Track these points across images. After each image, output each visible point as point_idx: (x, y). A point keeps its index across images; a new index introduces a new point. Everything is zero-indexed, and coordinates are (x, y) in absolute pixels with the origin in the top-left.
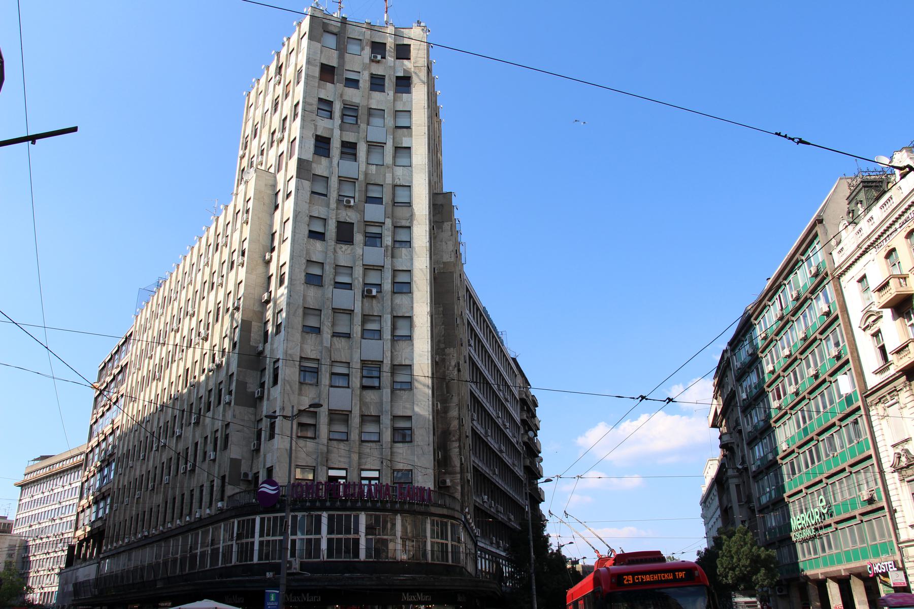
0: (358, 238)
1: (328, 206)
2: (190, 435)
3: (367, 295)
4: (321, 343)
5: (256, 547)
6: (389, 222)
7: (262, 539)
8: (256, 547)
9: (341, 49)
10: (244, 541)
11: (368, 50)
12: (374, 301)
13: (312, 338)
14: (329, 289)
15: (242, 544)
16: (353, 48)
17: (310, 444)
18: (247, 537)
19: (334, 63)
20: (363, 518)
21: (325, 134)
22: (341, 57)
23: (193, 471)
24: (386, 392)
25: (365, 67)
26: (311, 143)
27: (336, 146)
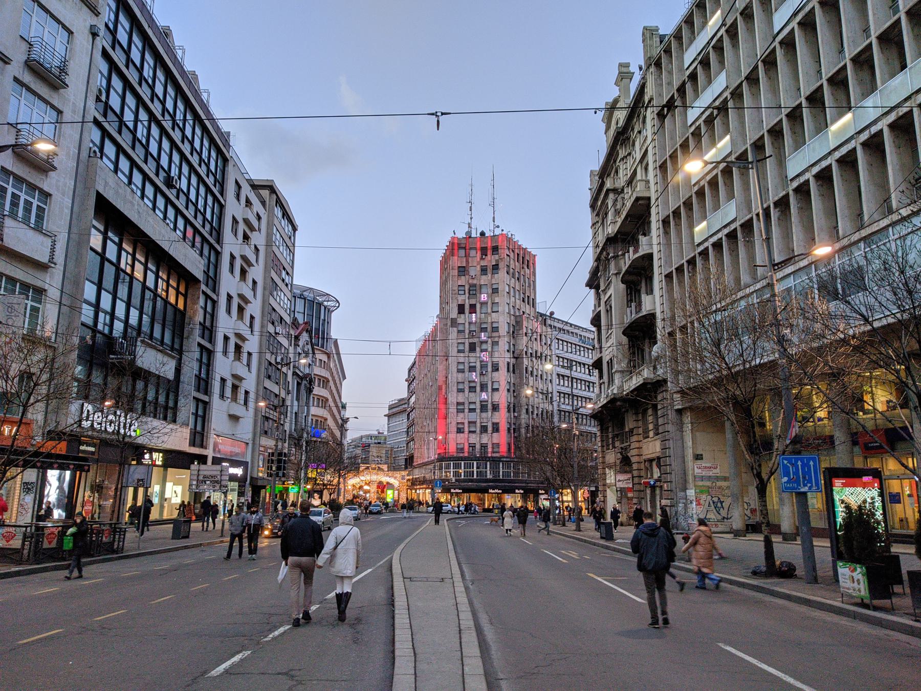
0: (478, 349)
3: (482, 374)
9: (467, 256)
11: (479, 253)
13: (461, 394)
14: (467, 373)
16: (473, 253)
19: (464, 265)
20: (475, 463)
22: (467, 262)
24: (490, 413)
25: (478, 263)
27: (467, 307)
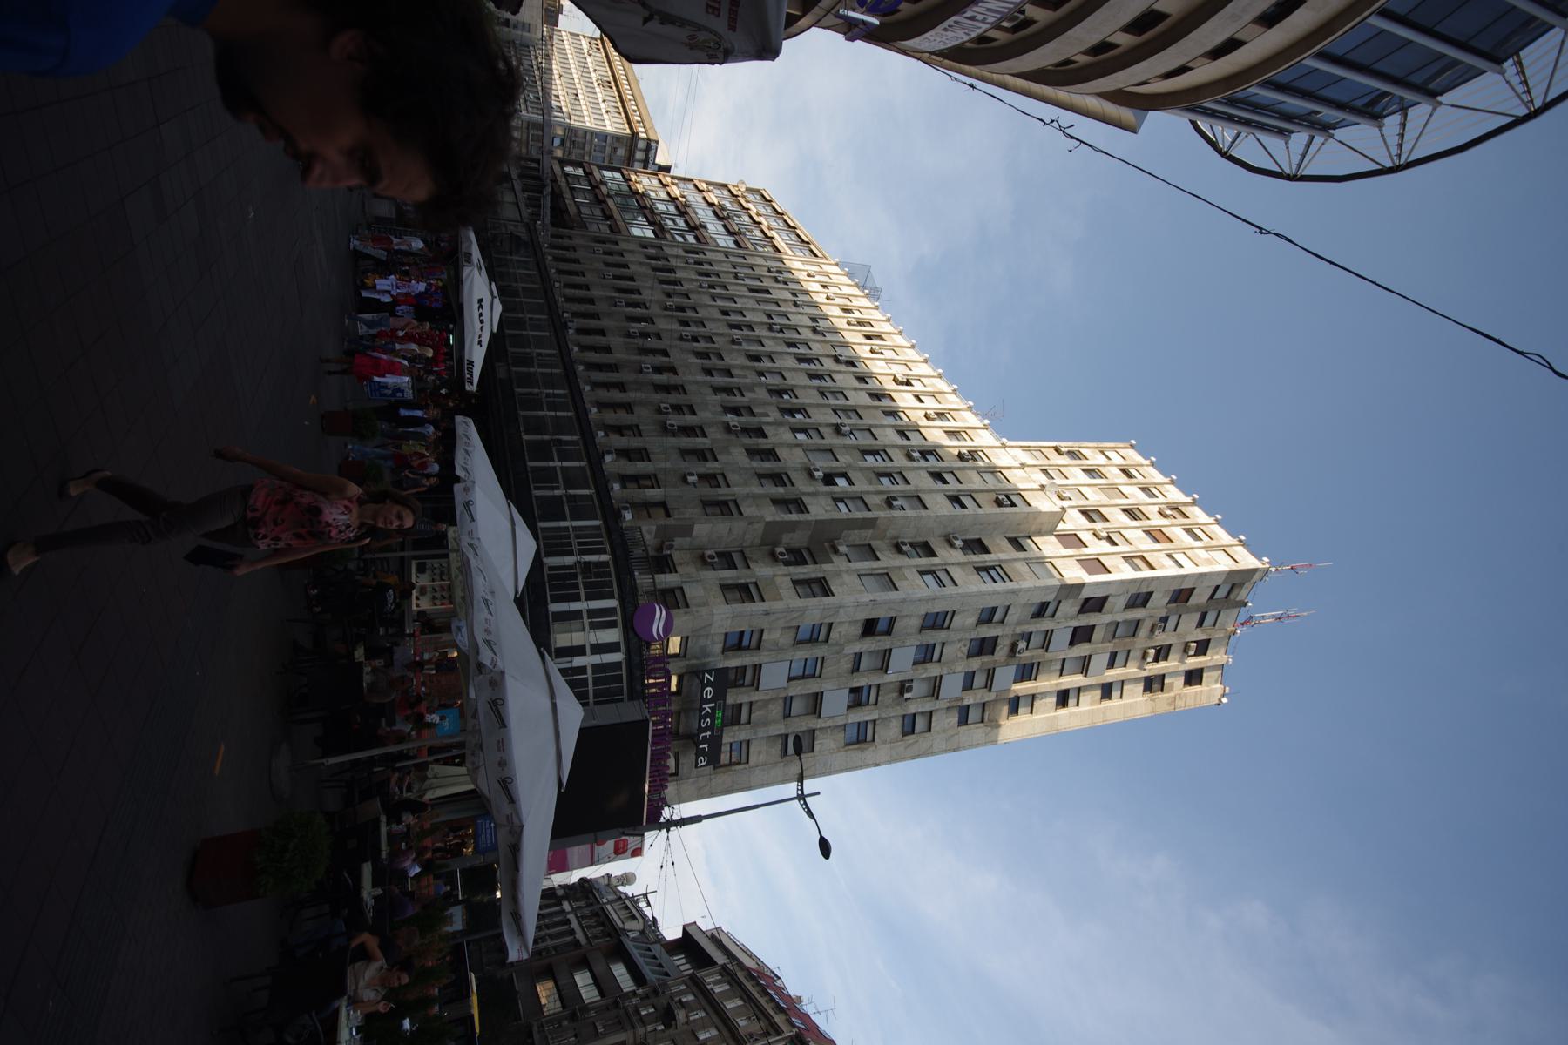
0: (975, 663)
1: (1019, 623)
2: (709, 410)
4: (849, 641)
5: (574, 606)
6: (991, 696)
7: (585, 614)
8: (574, 606)
10: (580, 579)
12: (895, 695)
13: (858, 630)
15: (575, 576)
17: (718, 647)
18: (586, 586)
21: (1107, 607)
23: (665, 430)
26: (1100, 593)
